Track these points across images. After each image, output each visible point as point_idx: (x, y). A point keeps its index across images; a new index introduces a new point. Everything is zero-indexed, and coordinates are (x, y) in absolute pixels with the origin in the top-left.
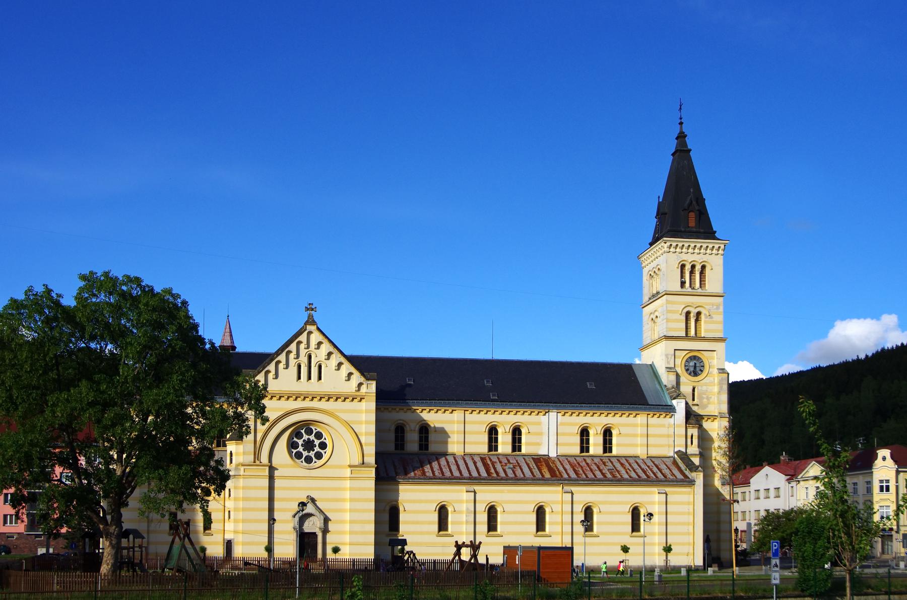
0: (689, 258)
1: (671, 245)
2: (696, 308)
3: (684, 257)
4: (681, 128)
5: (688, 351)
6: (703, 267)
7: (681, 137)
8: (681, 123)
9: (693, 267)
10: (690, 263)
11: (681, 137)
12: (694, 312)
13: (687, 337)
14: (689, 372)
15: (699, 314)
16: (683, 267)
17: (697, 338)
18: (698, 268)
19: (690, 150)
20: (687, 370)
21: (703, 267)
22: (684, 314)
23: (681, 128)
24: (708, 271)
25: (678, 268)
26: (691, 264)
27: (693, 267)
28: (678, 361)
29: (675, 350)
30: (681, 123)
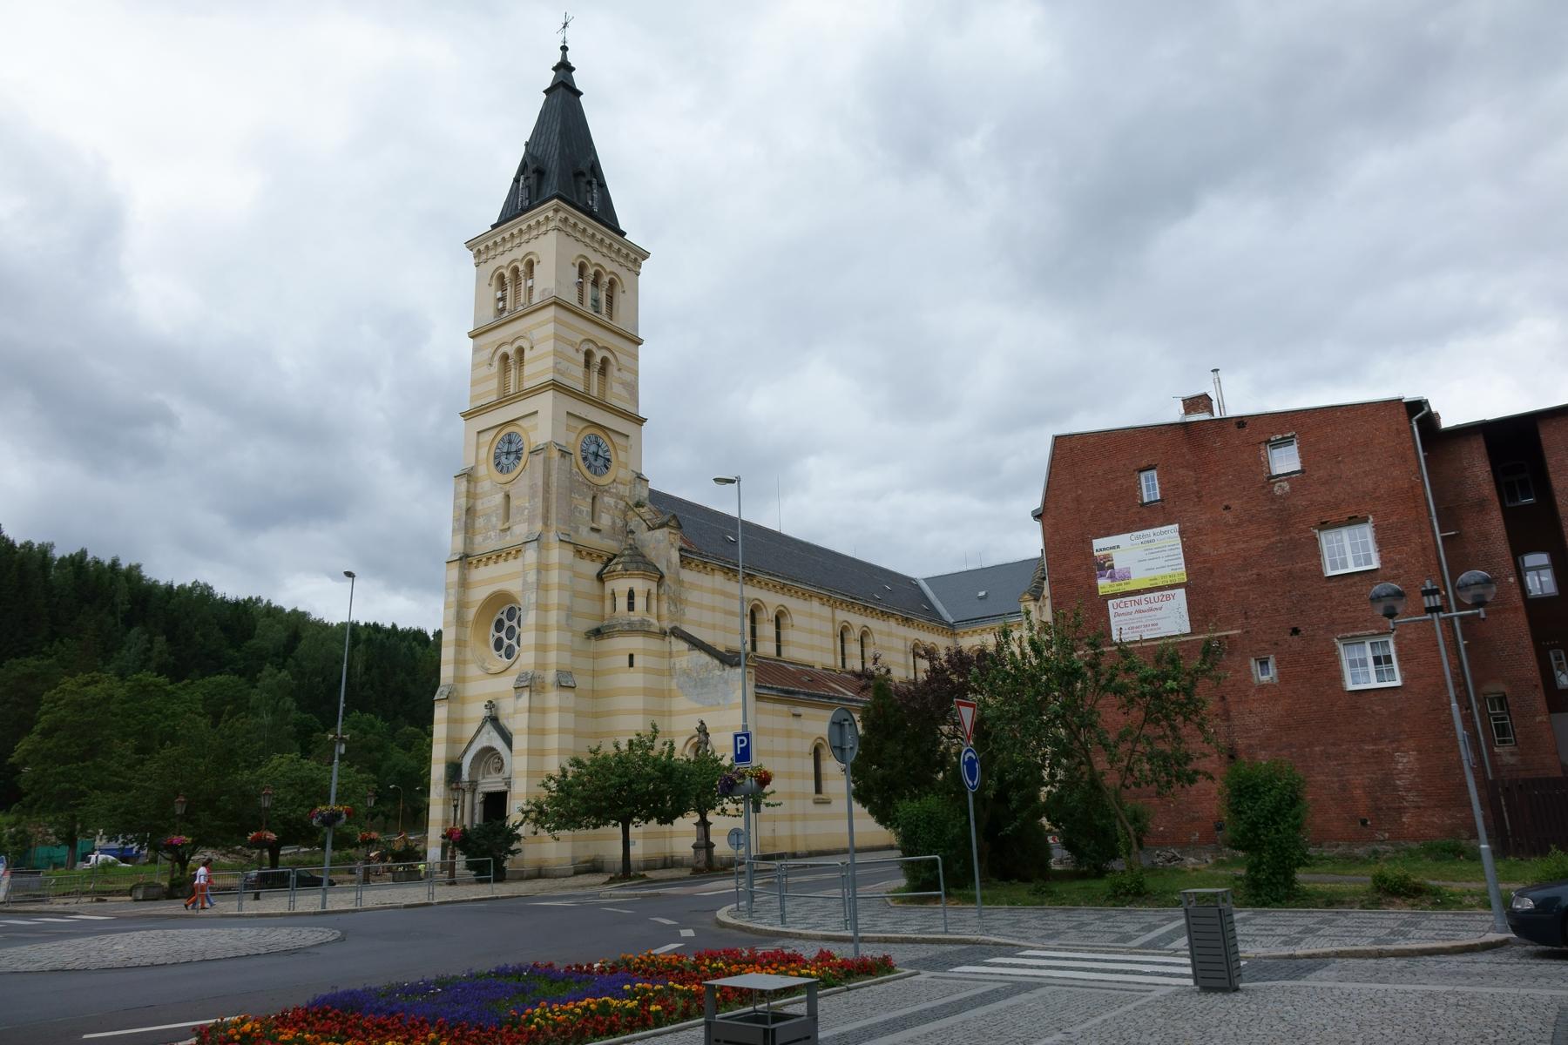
0: (503, 260)
2: (512, 343)
4: (564, 56)
5: (499, 428)
7: (564, 68)
8: (564, 49)
9: (516, 271)
11: (564, 68)
13: (505, 400)
14: (500, 466)
15: (521, 351)
23: (564, 56)
27: (516, 271)
28: (484, 452)
29: (479, 433)
30: (564, 49)
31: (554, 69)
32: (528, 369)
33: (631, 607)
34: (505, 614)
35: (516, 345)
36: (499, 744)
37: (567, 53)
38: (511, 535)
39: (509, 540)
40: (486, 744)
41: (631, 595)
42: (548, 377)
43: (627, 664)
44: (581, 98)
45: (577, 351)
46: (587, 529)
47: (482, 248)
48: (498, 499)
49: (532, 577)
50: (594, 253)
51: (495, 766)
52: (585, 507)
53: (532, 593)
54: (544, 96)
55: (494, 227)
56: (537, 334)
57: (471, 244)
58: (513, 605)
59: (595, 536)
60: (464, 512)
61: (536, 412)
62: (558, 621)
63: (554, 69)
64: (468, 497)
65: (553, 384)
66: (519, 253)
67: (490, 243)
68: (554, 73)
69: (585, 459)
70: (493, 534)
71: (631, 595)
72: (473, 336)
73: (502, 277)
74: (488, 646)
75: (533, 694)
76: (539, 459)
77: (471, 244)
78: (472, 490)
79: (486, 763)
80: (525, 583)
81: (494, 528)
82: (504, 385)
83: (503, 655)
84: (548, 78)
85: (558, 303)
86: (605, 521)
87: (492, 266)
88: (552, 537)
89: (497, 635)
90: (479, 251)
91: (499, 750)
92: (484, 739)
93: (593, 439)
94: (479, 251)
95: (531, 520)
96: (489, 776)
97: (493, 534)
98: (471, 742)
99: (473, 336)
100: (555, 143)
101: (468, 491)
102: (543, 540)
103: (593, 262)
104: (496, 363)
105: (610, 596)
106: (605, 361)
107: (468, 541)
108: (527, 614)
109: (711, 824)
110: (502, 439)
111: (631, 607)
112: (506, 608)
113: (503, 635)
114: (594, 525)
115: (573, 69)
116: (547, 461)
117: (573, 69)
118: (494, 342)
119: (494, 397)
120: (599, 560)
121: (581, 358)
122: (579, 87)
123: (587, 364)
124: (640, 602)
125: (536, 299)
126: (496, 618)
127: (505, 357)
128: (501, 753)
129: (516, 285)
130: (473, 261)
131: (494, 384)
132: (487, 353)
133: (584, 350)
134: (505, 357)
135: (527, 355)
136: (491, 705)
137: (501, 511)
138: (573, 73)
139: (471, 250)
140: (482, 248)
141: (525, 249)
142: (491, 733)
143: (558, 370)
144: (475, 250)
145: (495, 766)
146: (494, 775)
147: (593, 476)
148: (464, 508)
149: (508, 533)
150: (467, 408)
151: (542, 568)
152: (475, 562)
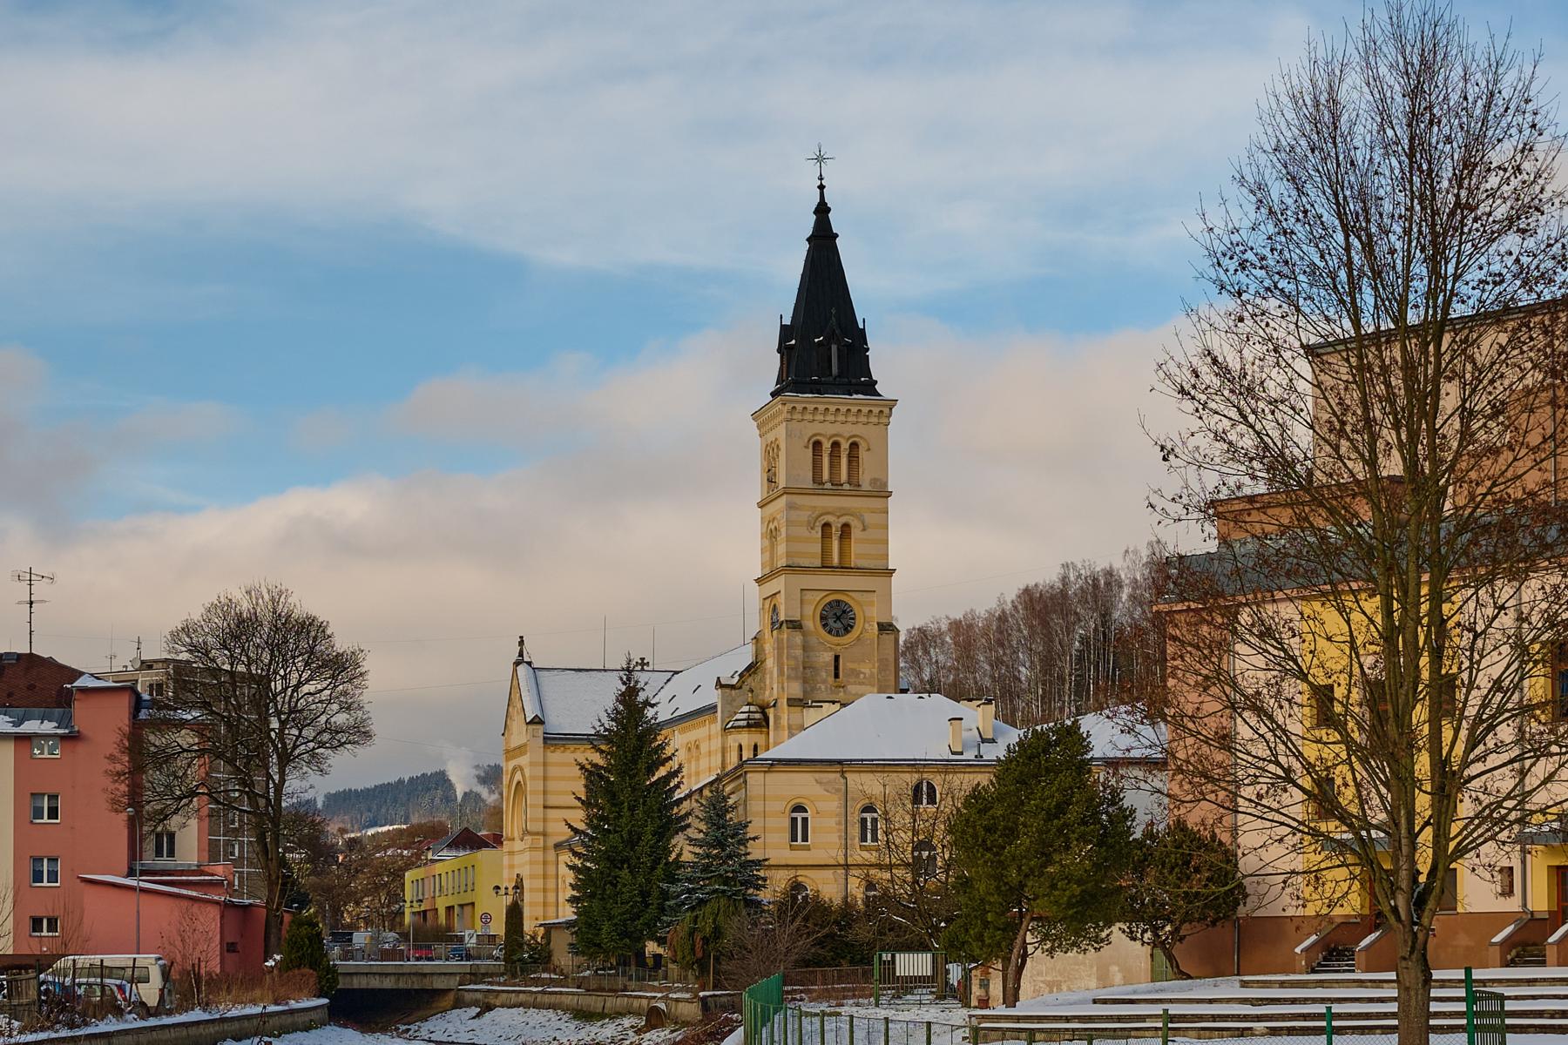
0: (829, 429)
1: (794, 408)
3: (817, 428)
6: (854, 446)
7: (822, 210)
8: (821, 187)
9: (836, 445)
11: (822, 210)
12: (836, 523)
13: (826, 566)
16: (817, 445)
17: (844, 568)
18: (845, 446)
19: (837, 236)
20: (824, 626)
21: (854, 446)
24: (862, 453)
25: (807, 447)
26: (850, 441)
27: (836, 445)
28: (809, 610)
30: (821, 187)
35: (844, 520)
38: (844, 692)
48: (828, 657)
73: (817, 445)
81: (824, 682)
82: (825, 552)
110: (830, 603)
125: (866, 486)
127: (826, 526)
132: (804, 516)
135: (856, 533)
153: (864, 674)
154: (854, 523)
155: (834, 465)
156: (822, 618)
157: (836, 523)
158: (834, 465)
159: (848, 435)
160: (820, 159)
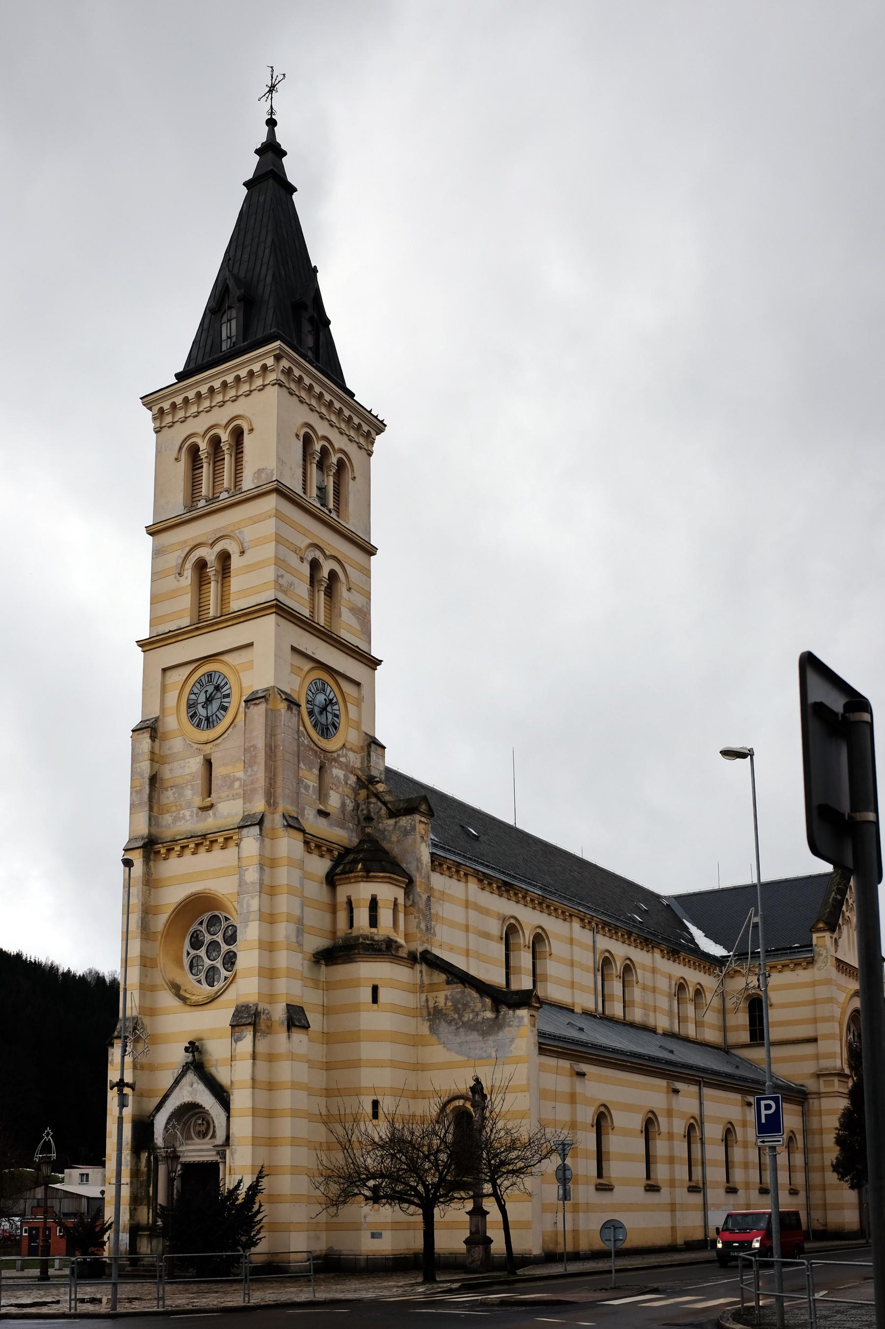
0: (199, 425)
2: (213, 544)
4: (272, 134)
8: (271, 123)
9: (216, 442)
10: (204, 436)
12: (210, 555)
14: (196, 720)
15: (225, 558)
21: (238, 435)
22: (188, 573)
23: (272, 134)
24: (247, 438)
25: (177, 459)
27: (216, 442)
29: (164, 670)
30: (271, 123)
31: (257, 152)
32: (236, 583)
33: (374, 922)
34: (205, 925)
35: (218, 547)
36: (207, 1100)
37: (276, 128)
38: (214, 814)
39: (209, 822)
40: (187, 1099)
41: (374, 904)
42: (269, 595)
43: (370, 1000)
44: (295, 197)
45: (302, 559)
46: (314, 812)
47: (166, 405)
48: (195, 764)
49: (252, 875)
50: (319, 419)
51: (198, 1128)
52: (311, 778)
53: (252, 897)
54: (245, 191)
55: (180, 377)
56: (248, 534)
57: (148, 401)
58: (217, 913)
59: (322, 822)
60: (147, 781)
61: (251, 645)
62: (287, 937)
63: (257, 152)
64: (152, 760)
65: (276, 606)
66: (222, 416)
67: (179, 400)
68: (258, 158)
69: (311, 713)
70: (187, 813)
71: (374, 904)
72: (153, 531)
73: (194, 451)
74: (181, 966)
75: (258, 1034)
76: (259, 711)
77: (148, 401)
78: (157, 751)
79: (185, 1124)
80: (241, 883)
81: (189, 806)
82: (200, 604)
83: (203, 981)
84: (249, 166)
85: (281, 491)
86: (334, 802)
87: (180, 433)
88: (278, 820)
89: (193, 952)
90: (161, 411)
91: (207, 1108)
92: (185, 1092)
93: (320, 686)
94: (161, 411)
95: (247, 797)
96: (189, 1142)
97: (187, 813)
98: (166, 1097)
99: (153, 531)
100: (266, 259)
101: (152, 752)
102: (267, 824)
103: (320, 434)
104: (188, 576)
105: (345, 906)
106: (333, 574)
107: (153, 823)
108: (246, 926)
109: (489, 1213)
110: (199, 681)
111: (374, 922)
112: (206, 917)
113: (202, 952)
114: (321, 807)
115: (284, 154)
116: (271, 717)
117: (284, 154)
118: (185, 542)
119: (185, 622)
120: (328, 856)
121: (306, 569)
122: (291, 178)
123: (313, 580)
124: (385, 916)
125: (248, 483)
126: (192, 930)
127: (201, 565)
128: (211, 1112)
129: (215, 462)
130: (151, 425)
131: (186, 601)
132: (173, 559)
133: (310, 559)
134: (201, 565)
135: (236, 562)
136: (193, 1047)
137: (199, 782)
138: (284, 160)
139: (150, 409)
140: (166, 405)
141: (231, 410)
142: (195, 1085)
143: (281, 586)
144: (156, 409)
145: (198, 1128)
146: (197, 1140)
147: (321, 738)
148: (147, 774)
149: (211, 812)
150: (145, 634)
151: (267, 863)
152: (163, 851)
153: (239, 779)
154: (232, 547)
155: (216, 475)
156: (191, 705)
157: (210, 555)
158: (216, 475)
159: (224, 422)
160: (272, 89)
